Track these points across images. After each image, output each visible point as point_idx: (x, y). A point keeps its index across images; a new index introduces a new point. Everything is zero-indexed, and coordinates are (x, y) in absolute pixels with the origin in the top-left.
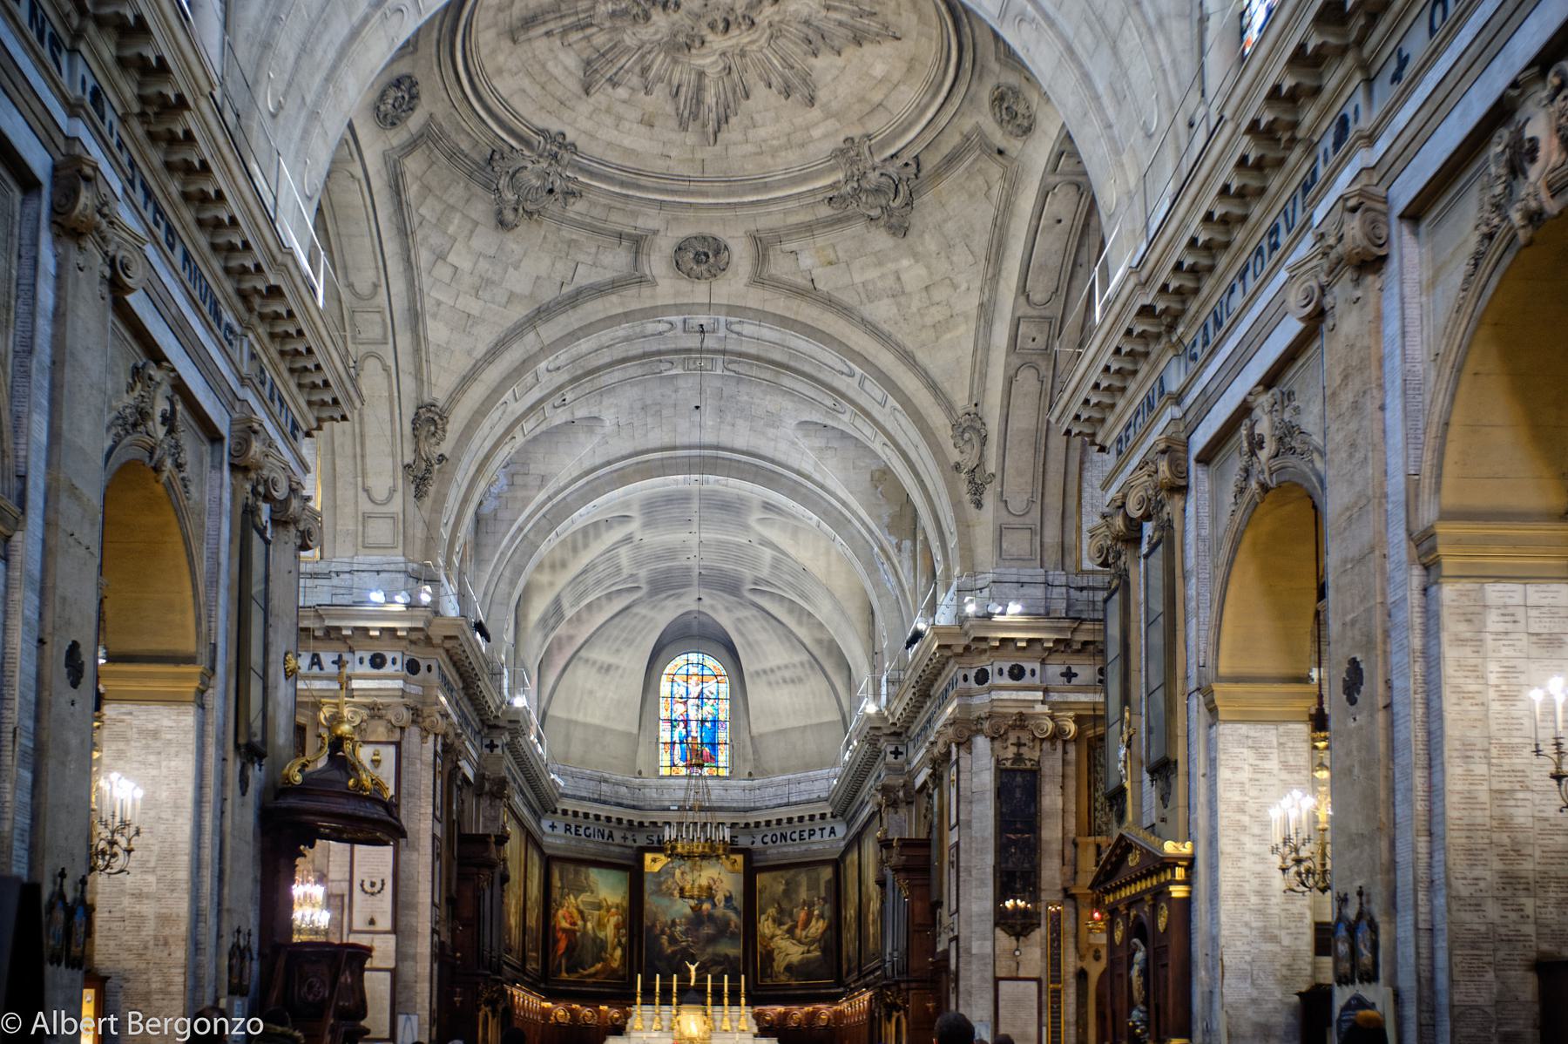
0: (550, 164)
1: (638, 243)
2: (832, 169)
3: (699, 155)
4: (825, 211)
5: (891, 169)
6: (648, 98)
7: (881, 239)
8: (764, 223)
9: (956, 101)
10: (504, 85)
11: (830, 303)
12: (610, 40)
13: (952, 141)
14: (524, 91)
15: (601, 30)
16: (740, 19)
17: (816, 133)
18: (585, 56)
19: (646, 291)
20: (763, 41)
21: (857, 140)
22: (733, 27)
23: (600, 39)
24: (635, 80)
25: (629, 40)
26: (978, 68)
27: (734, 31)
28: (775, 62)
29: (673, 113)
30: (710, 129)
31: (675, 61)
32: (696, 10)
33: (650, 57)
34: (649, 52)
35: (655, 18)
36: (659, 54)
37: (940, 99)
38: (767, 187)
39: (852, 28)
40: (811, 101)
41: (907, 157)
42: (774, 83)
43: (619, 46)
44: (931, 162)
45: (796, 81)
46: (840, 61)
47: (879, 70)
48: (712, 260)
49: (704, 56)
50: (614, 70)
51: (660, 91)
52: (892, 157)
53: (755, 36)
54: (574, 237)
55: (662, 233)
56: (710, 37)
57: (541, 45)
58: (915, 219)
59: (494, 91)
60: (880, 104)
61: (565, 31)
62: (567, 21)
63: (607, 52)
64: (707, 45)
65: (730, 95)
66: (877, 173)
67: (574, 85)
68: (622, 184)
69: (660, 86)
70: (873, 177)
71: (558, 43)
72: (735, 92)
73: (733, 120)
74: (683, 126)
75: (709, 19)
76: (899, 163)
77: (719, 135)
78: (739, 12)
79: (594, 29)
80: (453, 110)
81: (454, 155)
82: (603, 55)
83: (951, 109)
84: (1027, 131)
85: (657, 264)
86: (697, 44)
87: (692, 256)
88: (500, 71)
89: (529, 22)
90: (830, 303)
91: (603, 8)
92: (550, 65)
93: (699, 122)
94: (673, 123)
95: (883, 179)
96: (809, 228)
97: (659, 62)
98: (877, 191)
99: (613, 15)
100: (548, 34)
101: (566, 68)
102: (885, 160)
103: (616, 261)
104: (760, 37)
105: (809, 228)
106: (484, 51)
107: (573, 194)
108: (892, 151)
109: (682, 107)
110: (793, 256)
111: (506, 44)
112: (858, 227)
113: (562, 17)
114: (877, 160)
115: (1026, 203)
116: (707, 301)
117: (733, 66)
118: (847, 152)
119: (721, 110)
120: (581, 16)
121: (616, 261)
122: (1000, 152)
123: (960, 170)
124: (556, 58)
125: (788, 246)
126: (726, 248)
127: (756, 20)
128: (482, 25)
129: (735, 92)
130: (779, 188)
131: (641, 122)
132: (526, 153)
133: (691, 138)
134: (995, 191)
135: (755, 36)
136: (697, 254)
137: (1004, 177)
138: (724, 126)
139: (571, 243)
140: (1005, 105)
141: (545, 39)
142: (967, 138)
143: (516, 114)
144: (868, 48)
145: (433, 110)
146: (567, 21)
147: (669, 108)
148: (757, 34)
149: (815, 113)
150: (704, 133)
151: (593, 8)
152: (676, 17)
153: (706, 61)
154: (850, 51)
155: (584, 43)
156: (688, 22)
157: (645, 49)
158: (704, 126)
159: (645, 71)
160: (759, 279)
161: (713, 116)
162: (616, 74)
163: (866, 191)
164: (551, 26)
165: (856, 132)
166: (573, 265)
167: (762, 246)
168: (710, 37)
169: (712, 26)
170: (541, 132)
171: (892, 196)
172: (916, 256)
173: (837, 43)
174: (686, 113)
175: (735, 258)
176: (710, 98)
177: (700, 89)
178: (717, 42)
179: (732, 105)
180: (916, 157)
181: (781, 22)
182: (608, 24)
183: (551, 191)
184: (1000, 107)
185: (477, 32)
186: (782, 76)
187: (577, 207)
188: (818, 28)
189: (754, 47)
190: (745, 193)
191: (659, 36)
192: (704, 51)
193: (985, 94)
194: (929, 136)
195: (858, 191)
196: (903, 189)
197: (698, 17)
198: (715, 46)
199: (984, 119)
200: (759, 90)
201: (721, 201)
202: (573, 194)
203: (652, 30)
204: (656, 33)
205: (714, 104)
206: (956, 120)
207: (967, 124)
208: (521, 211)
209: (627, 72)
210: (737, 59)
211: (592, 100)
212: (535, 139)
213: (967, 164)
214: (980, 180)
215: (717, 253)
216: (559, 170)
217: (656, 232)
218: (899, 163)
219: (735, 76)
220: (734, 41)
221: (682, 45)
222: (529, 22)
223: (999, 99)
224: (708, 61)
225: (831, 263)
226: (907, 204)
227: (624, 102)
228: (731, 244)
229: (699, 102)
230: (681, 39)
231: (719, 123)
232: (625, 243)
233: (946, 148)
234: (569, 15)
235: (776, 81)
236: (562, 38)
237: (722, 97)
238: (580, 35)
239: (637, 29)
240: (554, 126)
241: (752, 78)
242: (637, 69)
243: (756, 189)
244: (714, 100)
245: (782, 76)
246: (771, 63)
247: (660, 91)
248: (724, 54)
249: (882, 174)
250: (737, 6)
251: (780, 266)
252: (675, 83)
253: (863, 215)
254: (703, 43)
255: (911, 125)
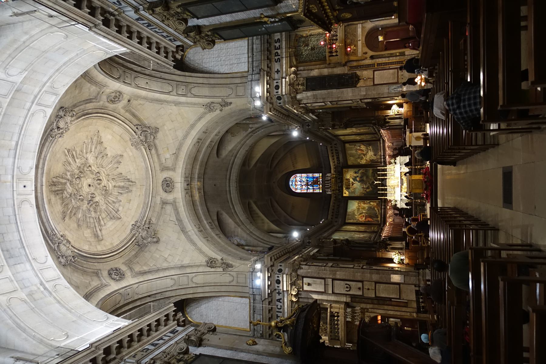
0: (140, 228)
1: (164, 203)
2: (141, 149)
3: (139, 187)
4: (153, 151)
5: (139, 133)
6: (122, 201)
7: (160, 135)
8: (158, 168)
9: (115, 114)
10: (116, 242)
11: (179, 149)
12: (104, 212)
13: (128, 115)
14: (118, 236)
15: (100, 215)
16: (97, 176)
17: (131, 154)
18: (109, 220)
19: (177, 201)
20: (104, 170)
21: (132, 143)
22: (99, 178)
23: (104, 215)
24: (117, 205)
25: (104, 207)
26: (103, 108)
27: (101, 178)
28: (110, 166)
29: (127, 194)
30: (131, 184)
31: (111, 194)
32: (94, 188)
33: (110, 201)
34: (108, 201)
35: (97, 200)
36: (109, 199)
37: (115, 119)
38: (147, 168)
39: (97, 144)
40: (121, 156)
41: (135, 128)
42: (117, 166)
43: (106, 210)
44: (136, 122)
45: (115, 160)
46: (108, 148)
47: (110, 137)
48: (168, 182)
49: (109, 186)
50: (113, 211)
51: (120, 198)
52: (135, 132)
53: (102, 172)
54: (162, 221)
55: (161, 196)
56: (103, 184)
57: (104, 232)
58: (153, 126)
59: (117, 245)
60: (120, 136)
61: (100, 225)
62: (97, 225)
63: (107, 213)
64: (105, 185)
65: (121, 178)
66: (140, 137)
67: (118, 222)
68: (147, 208)
69: (118, 198)
70: (142, 138)
71: (104, 227)
72: (120, 177)
73: (128, 177)
74: (131, 191)
75: (97, 185)
76: (137, 130)
77: (133, 181)
78: (94, 176)
79: (100, 217)
80: (122, 257)
81: (136, 256)
82: (109, 214)
83: (118, 116)
84: (120, 93)
85: (170, 197)
86: (105, 188)
87: (167, 188)
88: (112, 244)
89: (96, 236)
90: (179, 149)
91: (93, 215)
92: (111, 229)
93: (129, 187)
94: (130, 194)
95: (142, 135)
96: (158, 155)
97: (111, 199)
98: (146, 137)
99: (95, 212)
100: (100, 230)
101: (112, 224)
102: (136, 134)
103: (169, 209)
104: (102, 170)
105: (158, 155)
106: (105, 249)
107: (150, 222)
108: (133, 132)
109: (125, 192)
110: (166, 160)
111: (103, 242)
112: (157, 142)
113: (95, 227)
114: (137, 137)
115: (143, 93)
116: (180, 183)
117: (112, 178)
118: (135, 145)
119: (125, 181)
120: (95, 221)
121: (169, 209)
122: (129, 101)
123: (137, 113)
124: (109, 228)
125: (164, 161)
126: (165, 178)
127: (97, 172)
128: (95, 250)
129: (120, 177)
130: (147, 164)
131: (129, 203)
132: (136, 235)
133: (134, 189)
134: (141, 102)
135: (102, 172)
136: (167, 186)
137: (136, 100)
138: (130, 180)
139: (164, 222)
140: (113, 99)
141: (103, 231)
142: (127, 111)
143: (125, 239)
144: (103, 140)
145: (121, 263)
146: (97, 225)
147: (125, 195)
148: (101, 171)
149: (125, 154)
150: (132, 185)
151: (93, 218)
152: (96, 194)
153: (110, 185)
154: (105, 145)
155: (105, 220)
156: (98, 191)
157: (107, 202)
158: (130, 185)
159: (114, 202)
160: (173, 169)
161: (127, 183)
162: (114, 210)
163: (146, 140)
164: (98, 229)
165: (130, 143)
166: (170, 221)
167: (164, 169)
168: (103, 184)
169: (99, 184)
170: (132, 230)
171: (147, 132)
172: (164, 125)
173: (103, 149)
174: (127, 190)
175: (168, 176)
176: (122, 184)
177: (119, 187)
178: (104, 182)
179: (124, 178)
180: (134, 126)
181: (97, 165)
182: (99, 213)
183: (149, 228)
184: (115, 101)
185: (97, 251)
186: (114, 164)
187: (154, 220)
188: (98, 154)
189: (106, 172)
190: (149, 174)
191: (103, 199)
192: (107, 186)
193: (111, 106)
194: (127, 122)
195: (146, 142)
196: (144, 129)
197: (96, 188)
198: (106, 183)
199: (120, 105)
200: (119, 171)
201: (151, 180)
202: (150, 222)
203: (101, 201)
204: (102, 200)
205: (124, 183)
206: (121, 114)
207: (122, 111)
208: (154, 236)
209: (114, 207)
210: (110, 177)
211: (122, 217)
212: (133, 232)
213: (134, 111)
214: (139, 107)
215: (167, 181)
216: (142, 226)
217: (161, 198)
218: (137, 130)
219: (115, 177)
220: (104, 178)
221: (106, 192)
222: (96, 236)
223: (113, 102)
224: (110, 185)
225: (168, 149)
226: (149, 128)
227: (123, 208)
228: (164, 177)
229: (123, 187)
230: (104, 192)
231: (129, 181)
232: (164, 207)
233: (131, 117)
234: (95, 224)
235: (116, 166)
236: (102, 226)
237: (121, 180)
238: (102, 221)
239: (100, 205)
240: (130, 227)
241: (116, 173)
242: (113, 204)
243: (148, 170)
244: (122, 183)
245: (114, 164)
246: (110, 167)
247: (120, 198)
248: (108, 181)
249: (141, 135)
250: (92, 177)
251: (169, 164)
252: (117, 194)
253: (153, 140)
254: (105, 186)
255: (125, 127)
